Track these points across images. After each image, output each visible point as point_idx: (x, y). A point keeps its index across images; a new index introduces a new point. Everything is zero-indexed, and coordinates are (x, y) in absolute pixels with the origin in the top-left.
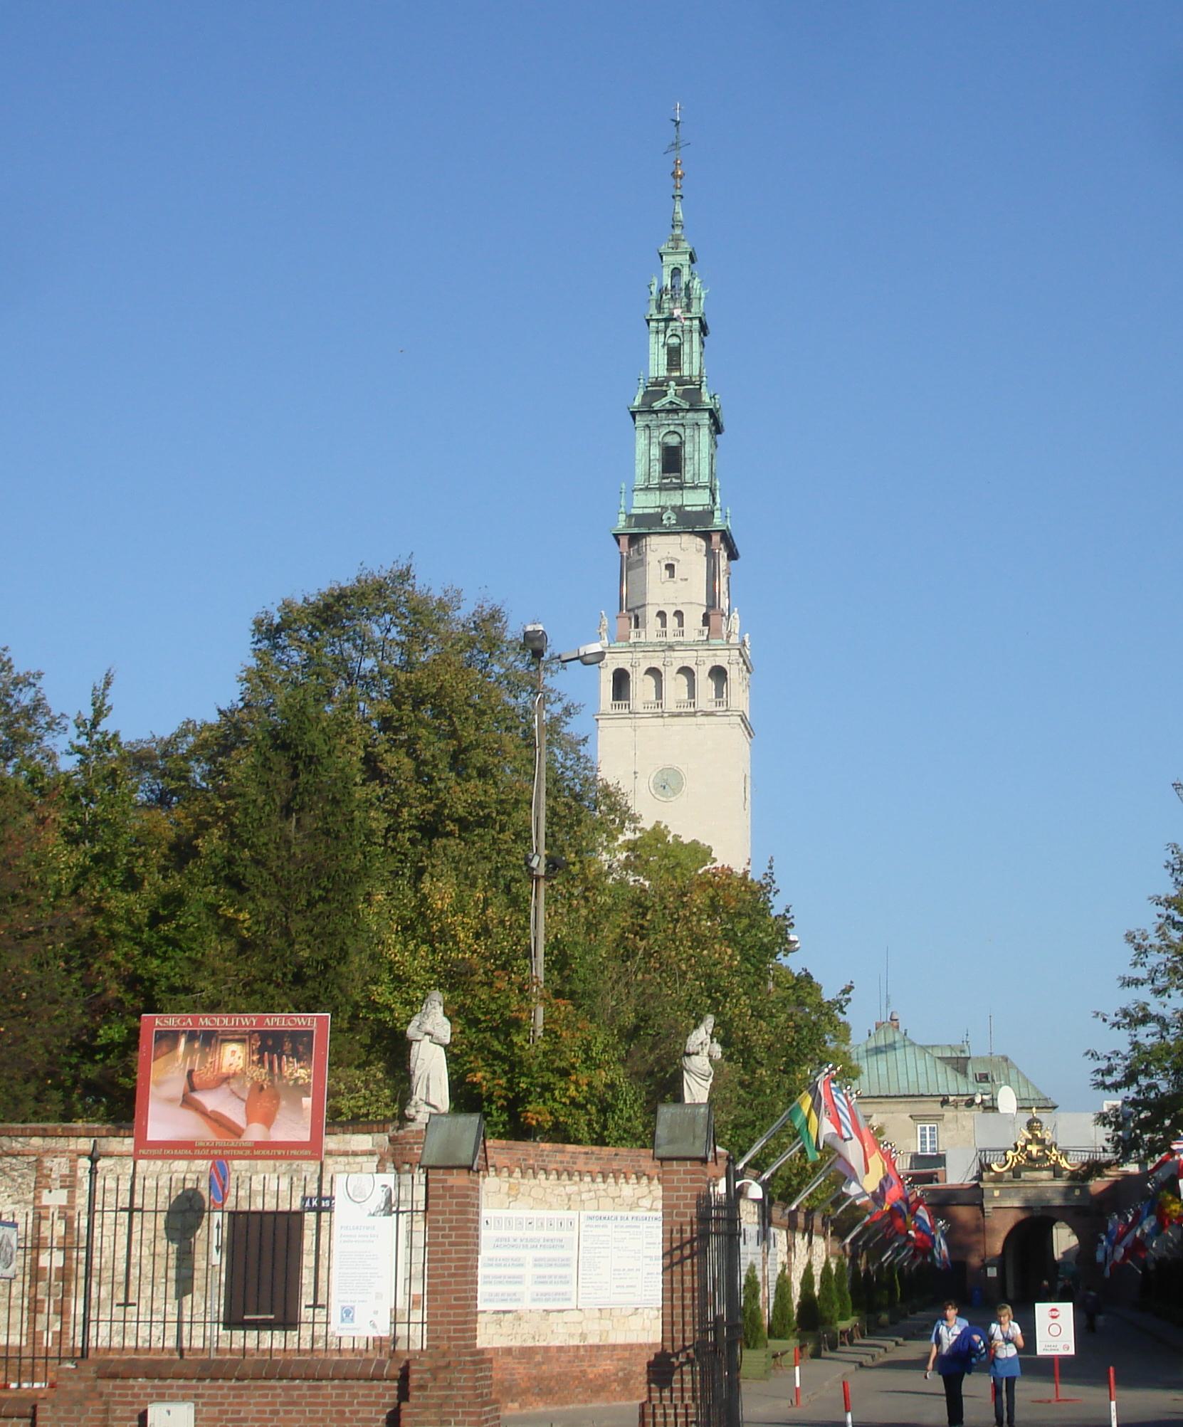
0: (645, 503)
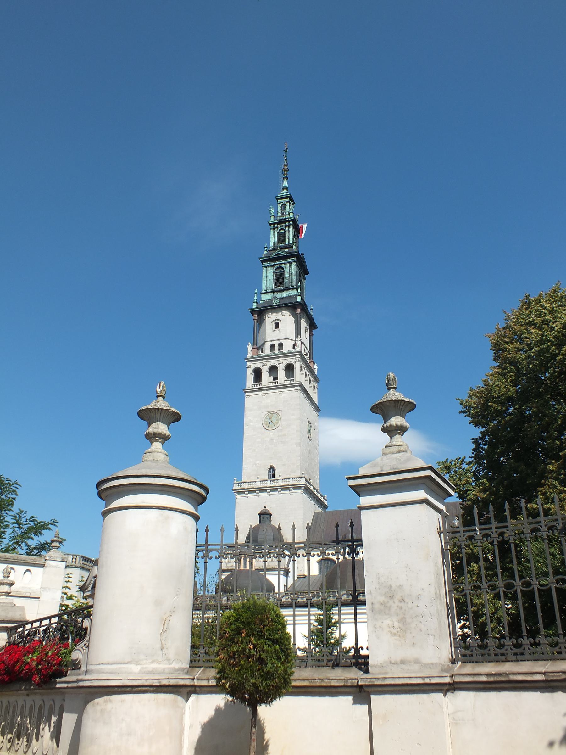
0: (266, 297)
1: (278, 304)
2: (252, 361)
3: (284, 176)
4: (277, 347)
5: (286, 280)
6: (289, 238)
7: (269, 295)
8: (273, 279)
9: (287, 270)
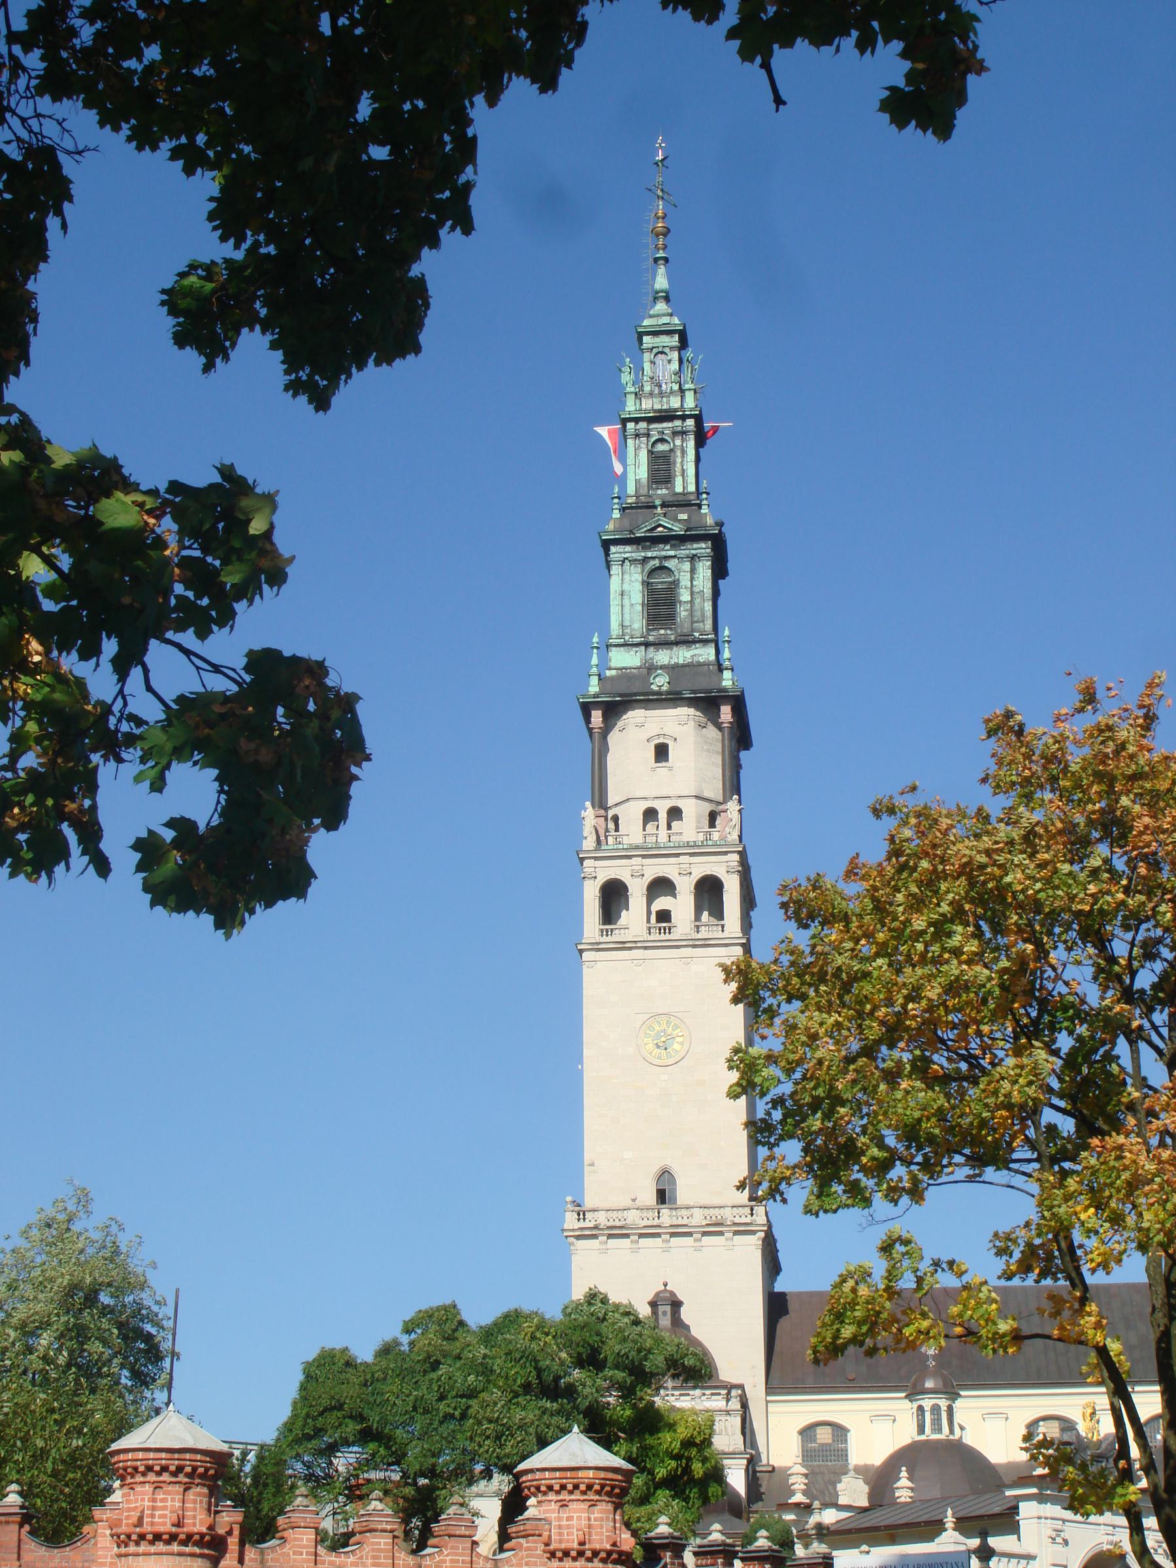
1: (664, 688)
2: (596, 858)
3: (658, 256)
4: (663, 816)
5: (682, 612)
6: (683, 471)
7: (632, 653)
9: (685, 580)
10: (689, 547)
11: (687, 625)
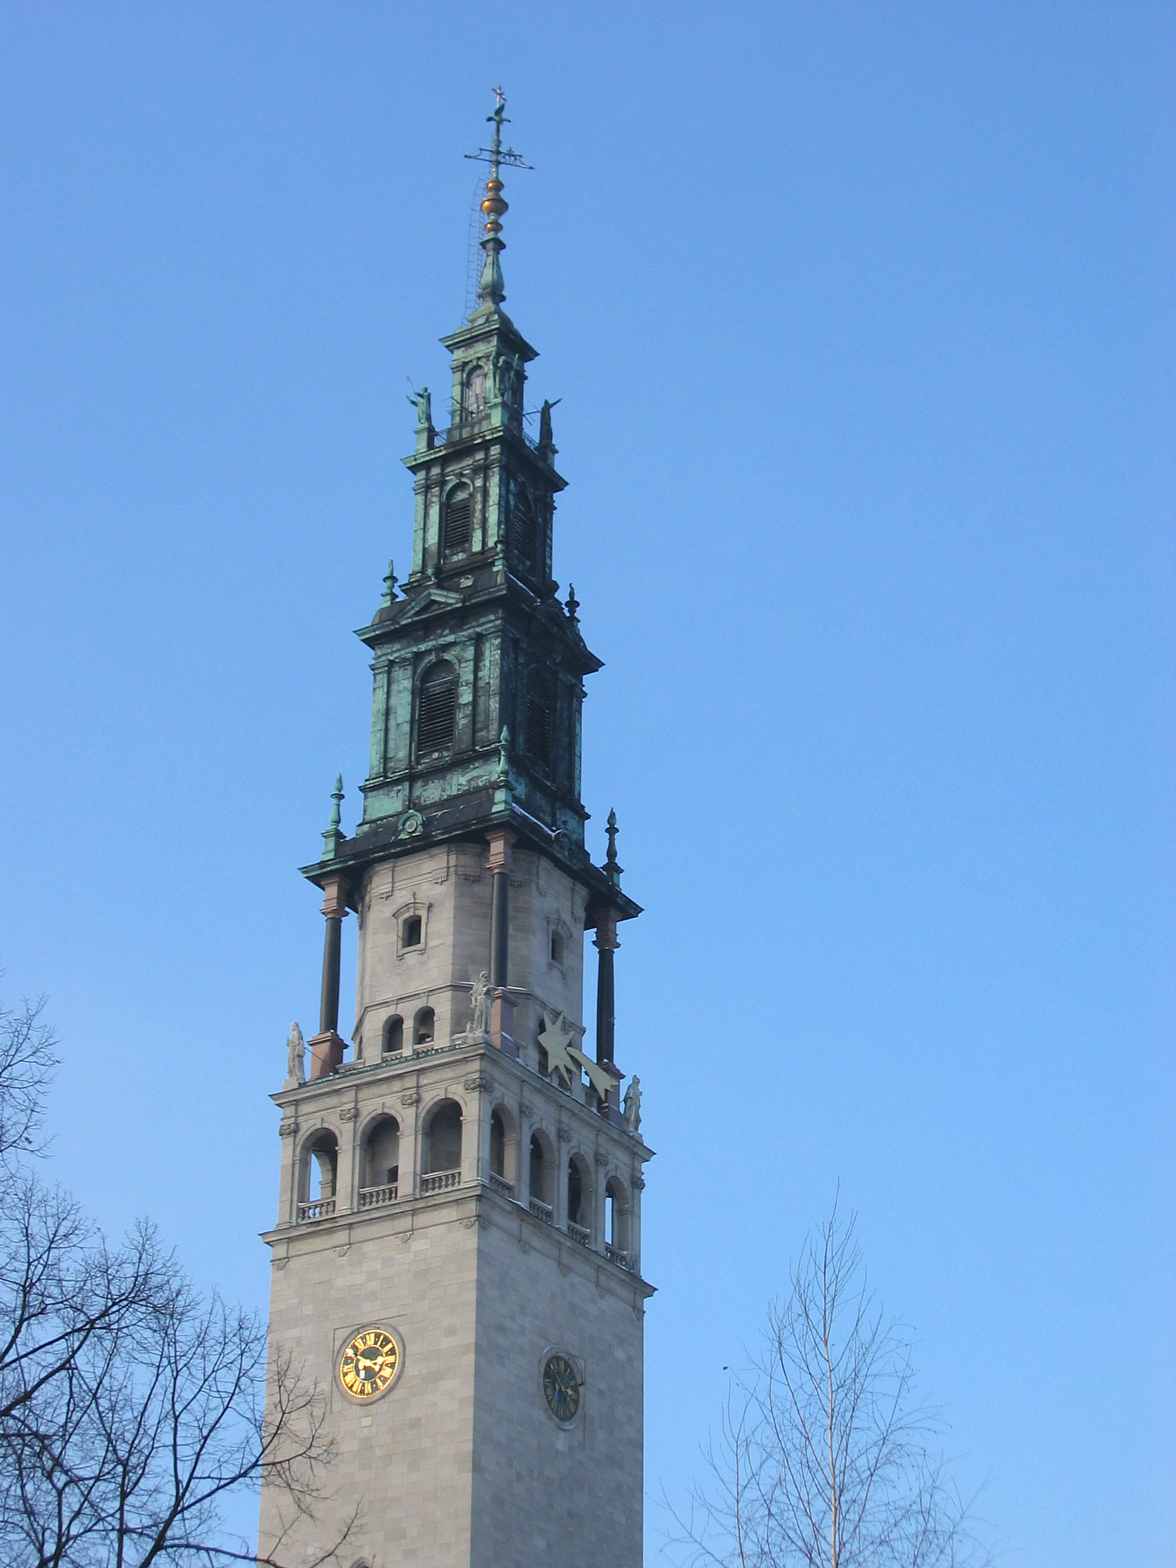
4: (408, 1026)
5: (462, 720)
6: (484, 520)
7: (393, 794)
8: (412, 722)
9: (467, 675)
10: (474, 624)
11: (466, 738)
